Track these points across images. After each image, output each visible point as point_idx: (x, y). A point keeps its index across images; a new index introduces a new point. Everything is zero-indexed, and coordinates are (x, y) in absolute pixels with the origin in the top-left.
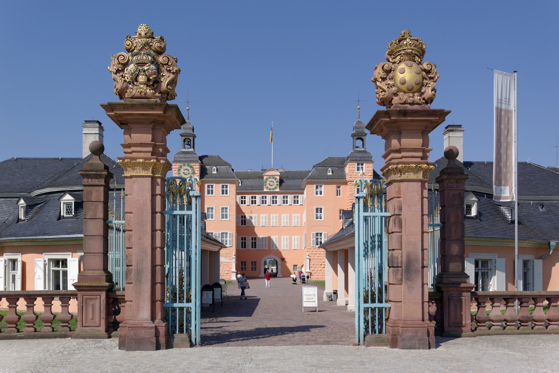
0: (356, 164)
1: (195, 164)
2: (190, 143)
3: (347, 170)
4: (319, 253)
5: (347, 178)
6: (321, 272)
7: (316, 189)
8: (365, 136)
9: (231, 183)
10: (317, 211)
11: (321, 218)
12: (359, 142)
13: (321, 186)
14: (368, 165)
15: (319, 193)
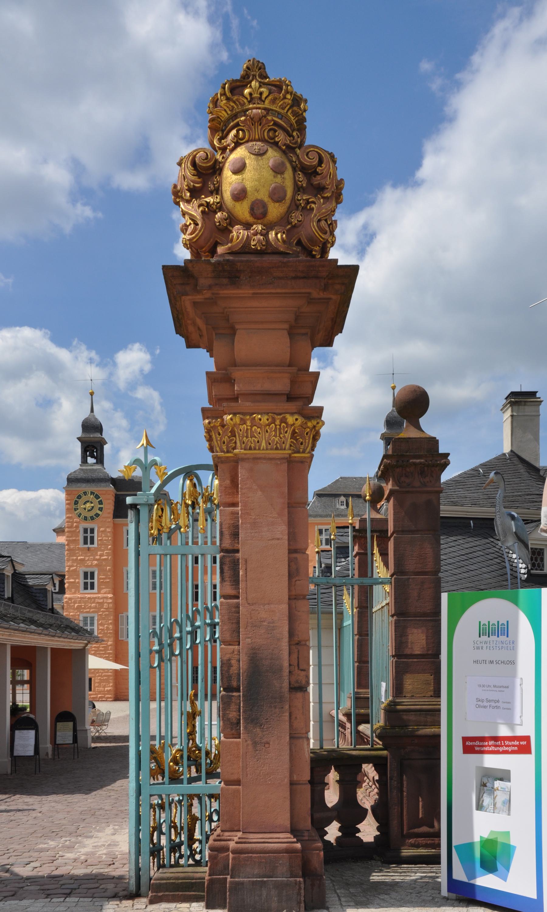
2: (95, 453)
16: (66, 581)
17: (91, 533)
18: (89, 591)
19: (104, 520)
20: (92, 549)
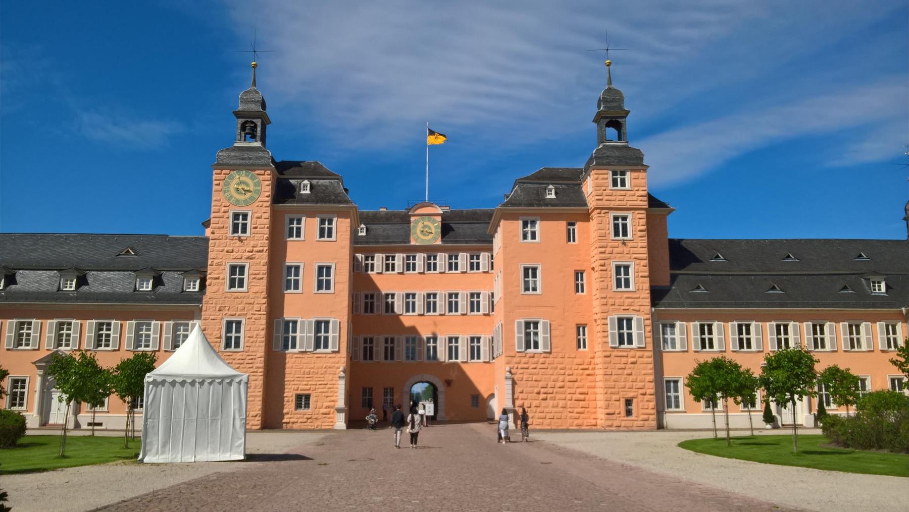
0: (610, 173)
1: (262, 172)
3: (589, 187)
4: (534, 366)
5: (589, 205)
6: (538, 409)
7: (524, 228)
8: (625, 117)
9: (342, 214)
10: (526, 275)
11: (534, 289)
12: (611, 132)
13: (533, 223)
14: (635, 174)
15: (529, 235)
16: (207, 278)
17: (243, 220)
18: (236, 289)
19: (261, 204)
20: (242, 238)
